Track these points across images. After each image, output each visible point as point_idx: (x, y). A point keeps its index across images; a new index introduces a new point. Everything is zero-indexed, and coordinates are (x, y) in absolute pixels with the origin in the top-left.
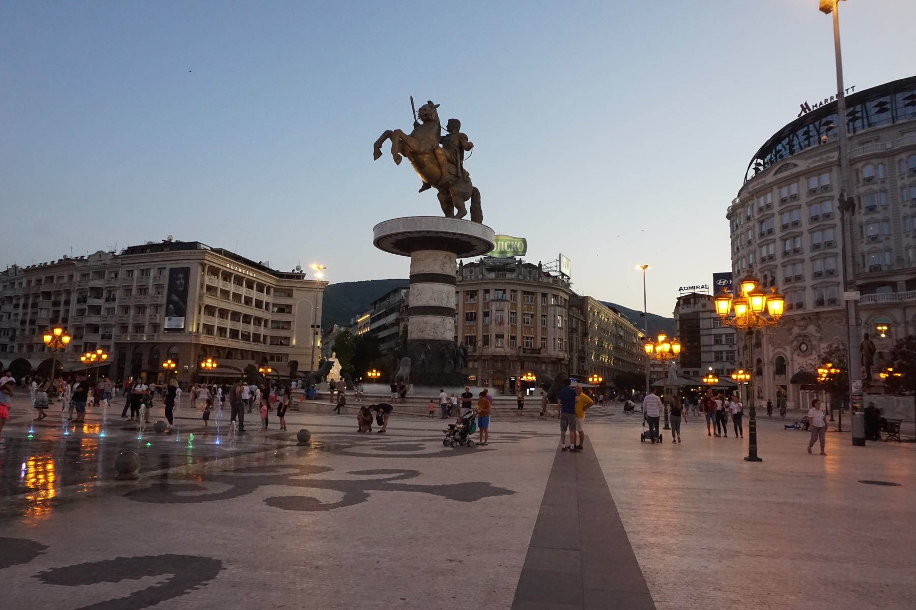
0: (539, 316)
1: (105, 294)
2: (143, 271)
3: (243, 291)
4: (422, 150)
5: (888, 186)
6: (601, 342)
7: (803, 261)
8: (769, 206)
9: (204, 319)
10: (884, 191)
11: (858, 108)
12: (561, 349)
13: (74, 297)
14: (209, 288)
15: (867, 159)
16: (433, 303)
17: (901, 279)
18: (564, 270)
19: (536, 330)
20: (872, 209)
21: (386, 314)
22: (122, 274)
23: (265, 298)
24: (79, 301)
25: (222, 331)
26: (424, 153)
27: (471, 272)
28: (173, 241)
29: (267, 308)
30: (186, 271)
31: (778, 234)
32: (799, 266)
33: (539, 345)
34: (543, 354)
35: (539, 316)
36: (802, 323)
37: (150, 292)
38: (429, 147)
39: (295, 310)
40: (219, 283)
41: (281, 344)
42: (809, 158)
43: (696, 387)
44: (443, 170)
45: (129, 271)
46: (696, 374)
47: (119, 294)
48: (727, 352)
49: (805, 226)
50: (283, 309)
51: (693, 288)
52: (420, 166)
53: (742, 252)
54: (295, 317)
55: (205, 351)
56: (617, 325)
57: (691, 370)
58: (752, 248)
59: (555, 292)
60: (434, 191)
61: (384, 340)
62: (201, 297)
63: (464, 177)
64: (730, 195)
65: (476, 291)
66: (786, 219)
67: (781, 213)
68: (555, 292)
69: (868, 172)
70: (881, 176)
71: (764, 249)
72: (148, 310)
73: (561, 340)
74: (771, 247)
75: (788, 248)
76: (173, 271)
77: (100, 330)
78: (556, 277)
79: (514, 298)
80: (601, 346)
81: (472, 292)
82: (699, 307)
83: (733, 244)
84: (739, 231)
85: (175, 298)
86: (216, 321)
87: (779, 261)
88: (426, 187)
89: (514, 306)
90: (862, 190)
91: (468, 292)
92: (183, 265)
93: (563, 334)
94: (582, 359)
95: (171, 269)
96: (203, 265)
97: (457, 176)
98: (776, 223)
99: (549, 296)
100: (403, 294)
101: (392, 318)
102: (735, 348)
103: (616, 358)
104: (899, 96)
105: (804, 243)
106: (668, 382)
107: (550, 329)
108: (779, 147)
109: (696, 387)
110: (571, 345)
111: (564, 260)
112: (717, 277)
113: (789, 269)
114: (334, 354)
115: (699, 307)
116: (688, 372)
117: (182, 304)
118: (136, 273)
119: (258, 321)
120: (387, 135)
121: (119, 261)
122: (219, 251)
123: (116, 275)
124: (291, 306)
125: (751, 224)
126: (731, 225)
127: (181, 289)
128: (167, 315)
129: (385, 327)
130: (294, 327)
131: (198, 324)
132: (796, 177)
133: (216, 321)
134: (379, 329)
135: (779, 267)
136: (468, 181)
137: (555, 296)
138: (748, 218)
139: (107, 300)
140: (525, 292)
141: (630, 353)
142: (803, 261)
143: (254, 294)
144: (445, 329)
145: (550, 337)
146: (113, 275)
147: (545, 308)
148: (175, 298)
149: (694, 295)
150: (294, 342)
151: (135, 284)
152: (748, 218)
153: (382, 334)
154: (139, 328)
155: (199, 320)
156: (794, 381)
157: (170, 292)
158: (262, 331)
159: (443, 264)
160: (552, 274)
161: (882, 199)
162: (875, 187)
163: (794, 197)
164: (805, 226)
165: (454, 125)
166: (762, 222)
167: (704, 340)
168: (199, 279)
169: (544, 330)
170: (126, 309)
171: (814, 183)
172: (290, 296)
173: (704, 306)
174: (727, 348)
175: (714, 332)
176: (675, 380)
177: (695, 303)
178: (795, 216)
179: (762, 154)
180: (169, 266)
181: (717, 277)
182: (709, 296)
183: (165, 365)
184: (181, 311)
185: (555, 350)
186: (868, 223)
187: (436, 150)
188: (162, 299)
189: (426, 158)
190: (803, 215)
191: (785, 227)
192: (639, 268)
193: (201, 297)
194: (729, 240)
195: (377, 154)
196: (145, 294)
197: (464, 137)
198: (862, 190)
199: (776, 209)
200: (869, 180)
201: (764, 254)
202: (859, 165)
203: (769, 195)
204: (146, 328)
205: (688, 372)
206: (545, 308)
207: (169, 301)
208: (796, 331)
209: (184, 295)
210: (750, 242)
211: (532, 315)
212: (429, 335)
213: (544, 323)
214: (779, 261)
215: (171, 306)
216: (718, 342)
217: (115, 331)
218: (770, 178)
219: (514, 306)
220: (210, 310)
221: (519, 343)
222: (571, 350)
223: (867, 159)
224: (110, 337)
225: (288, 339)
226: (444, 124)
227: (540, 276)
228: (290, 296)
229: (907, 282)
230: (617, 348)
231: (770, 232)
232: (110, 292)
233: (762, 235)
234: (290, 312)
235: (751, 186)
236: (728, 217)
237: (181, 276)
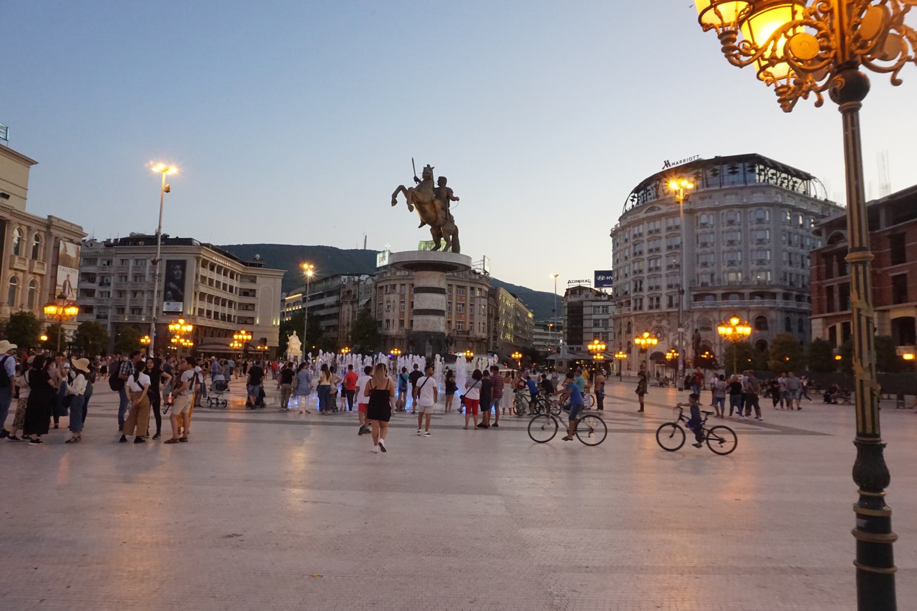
0: (468, 305)
1: (98, 279)
2: (137, 260)
3: (222, 279)
4: (426, 200)
5: (714, 229)
6: (506, 323)
7: (661, 276)
8: (640, 235)
9: (199, 304)
10: (712, 233)
11: (700, 171)
12: (484, 332)
14: (203, 278)
15: (703, 210)
16: (432, 308)
17: (719, 292)
18: (487, 269)
20: (704, 245)
21: (321, 296)
22: (116, 261)
23: (235, 284)
26: (425, 204)
29: (231, 291)
30: (183, 264)
31: (646, 255)
32: (659, 279)
33: (468, 328)
34: (471, 335)
35: (468, 305)
36: (659, 318)
37: (147, 279)
39: (258, 294)
40: (206, 272)
41: (246, 323)
42: (667, 204)
43: (579, 360)
44: (440, 216)
45: (123, 260)
46: (579, 349)
47: (113, 280)
48: (603, 333)
49: (664, 252)
50: (246, 293)
51: (579, 281)
52: (422, 212)
53: (620, 264)
54: (258, 300)
56: (517, 308)
57: (575, 347)
58: (627, 262)
59: (480, 286)
60: (428, 227)
61: (323, 318)
62: (197, 285)
63: (449, 219)
64: (614, 222)
66: (652, 245)
67: (648, 241)
69: (704, 219)
70: (711, 223)
71: (636, 264)
72: (146, 295)
74: (641, 263)
75: (652, 265)
76: (170, 263)
77: (95, 311)
78: (479, 273)
79: (451, 291)
80: (506, 327)
82: (583, 297)
83: (614, 256)
84: (619, 248)
85: (173, 285)
86: (205, 306)
87: (646, 274)
88: (422, 224)
89: (450, 297)
90: (700, 231)
92: (181, 258)
93: (485, 319)
94: (495, 338)
95: (168, 261)
96: (198, 259)
97: (446, 219)
98: (645, 247)
99: (477, 289)
101: (331, 300)
102: (610, 330)
103: (516, 337)
104: (725, 167)
105: (662, 263)
106: (560, 356)
107: (476, 316)
108: (649, 188)
109: (579, 360)
110: (489, 327)
111: (486, 260)
112: (598, 273)
113: (652, 280)
114: (295, 332)
115: (583, 297)
116: (573, 349)
117: (180, 291)
118: (131, 263)
119: (231, 303)
120: (401, 188)
121: (112, 250)
122: (207, 245)
123: (109, 263)
124: (255, 291)
125: (628, 244)
126: (613, 241)
127: (179, 278)
128: (165, 300)
129: (322, 307)
130: (258, 308)
131: (194, 309)
132: (659, 217)
133: (205, 306)
134: (312, 308)
135: (646, 279)
136: (452, 222)
137: (480, 290)
138: (626, 240)
139: (101, 284)
140: (458, 286)
141: (524, 332)
142: (661, 276)
143: (228, 281)
144: (438, 325)
145: (476, 322)
146: (105, 262)
147: (473, 299)
148: (173, 285)
149: (580, 288)
150: (258, 322)
151: (130, 273)
152: (626, 240)
153: (322, 313)
154: (136, 310)
156: (651, 358)
157: (168, 280)
158: (233, 312)
159: (440, 281)
160: (477, 271)
161: (711, 239)
162: (707, 230)
163: (658, 231)
164: (664, 252)
165: (442, 180)
166: (635, 245)
167: (586, 324)
168: (193, 270)
169: (472, 316)
170: (121, 293)
171: (671, 222)
173: (587, 296)
174: (603, 330)
175: (594, 317)
176: (565, 355)
177: (580, 294)
178: (657, 244)
179: (637, 190)
181: (598, 273)
182: (591, 289)
183: (143, 341)
184: (179, 298)
185: (480, 332)
186: (701, 254)
187: (431, 199)
188: (159, 286)
189: (427, 207)
190: (663, 244)
191: (650, 251)
192: (552, 276)
193: (197, 285)
194: (611, 253)
195: (394, 202)
196: (140, 281)
197: (450, 191)
198: (700, 231)
199: (646, 237)
200: (704, 225)
201: (636, 268)
202: (699, 214)
203: (641, 226)
205: (573, 349)
206: (473, 299)
207: (167, 288)
208: (654, 323)
209: (181, 284)
210: (626, 258)
211: (463, 305)
212: (430, 328)
213: (471, 310)
214: (646, 274)
215: (169, 293)
216: (596, 325)
217: (110, 313)
218: (642, 215)
219: (450, 297)
220: (202, 296)
221: (453, 327)
222: (489, 331)
223: (703, 210)
224: (106, 317)
225: (253, 319)
226: (436, 180)
228: (253, 280)
229: (723, 294)
230: (516, 328)
231: (641, 253)
232: (103, 277)
233: (635, 254)
235: (629, 218)
236: (611, 235)
237: (178, 267)
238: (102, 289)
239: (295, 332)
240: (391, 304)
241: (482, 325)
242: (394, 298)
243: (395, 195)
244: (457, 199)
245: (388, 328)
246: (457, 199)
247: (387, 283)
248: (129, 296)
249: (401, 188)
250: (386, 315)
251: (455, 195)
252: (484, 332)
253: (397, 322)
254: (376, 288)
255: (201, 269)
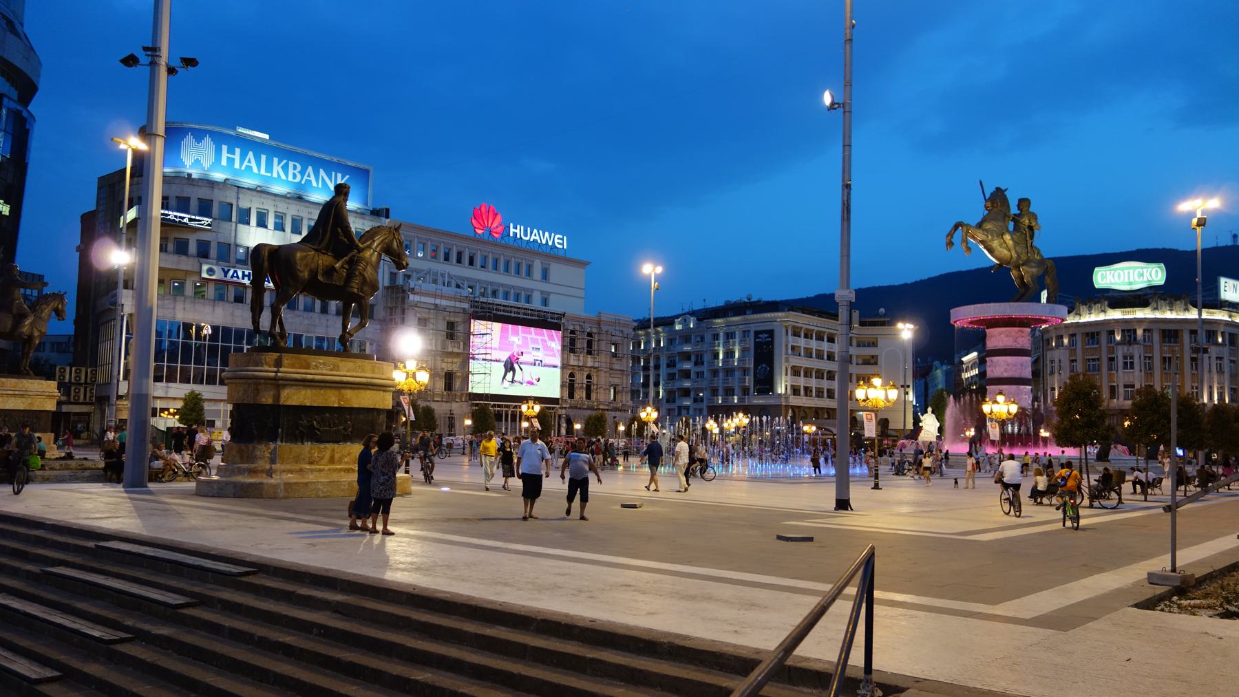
1: (693, 358)
13: (663, 362)
19: (1183, 377)
24: (668, 366)
25: (807, 390)
28: (754, 299)
39: (881, 361)
55: (801, 414)
65: (1098, 333)
76: (757, 333)
81: (1093, 334)
86: (802, 382)
91: (1087, 334)
114: (930, 409)
133: (802, 382)
172: (874, 344)
180: (753, 328)
204: (736, 391)
234: (876, 363)
238: (699, 369)
239: (930, 409)
240: (1056, 365)
243: (951, 235)
248: (721, 375)
255: (790, 338)
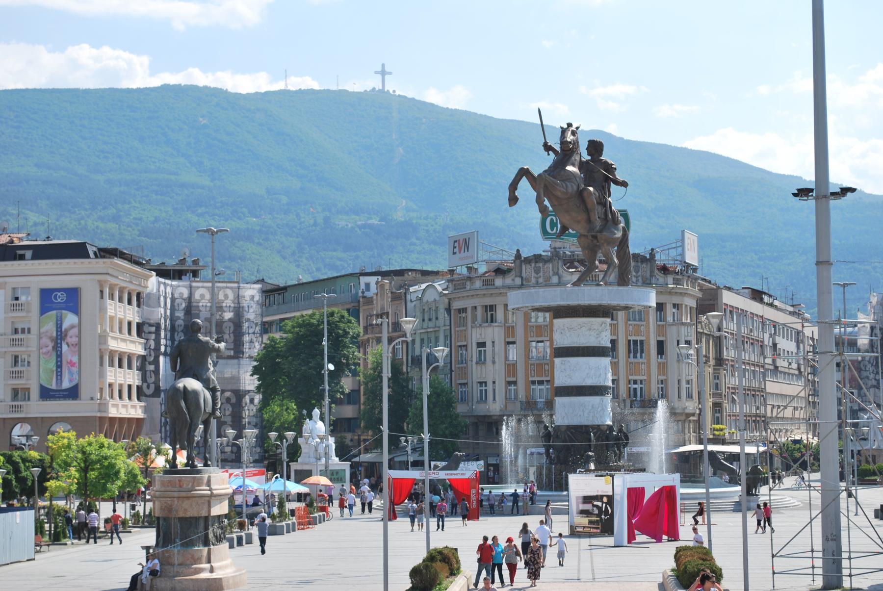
16: (589, 382)
27: (537, 271)
38: (575, 187)
59: (676, 300)
68: (676, 300)
73: (688, 382)
97: (606, 219)
100: (363, 286)
137: (676, 306)
155: (102, 375)
165: (595, 147)
195: (513, 200)
197: (609, 168)
227: (652, 272)
241: (684, 386)
242: (493, 334)
243: (514, 186)
244: (624, 184)
245: (483, 399)
246: (624, 184)
247: (476, 302)
249: (524, 173)
250: (476, 373)
251: (619, 176)
252: (689, 396)
253: (500, 387)
254: (449, 310)
